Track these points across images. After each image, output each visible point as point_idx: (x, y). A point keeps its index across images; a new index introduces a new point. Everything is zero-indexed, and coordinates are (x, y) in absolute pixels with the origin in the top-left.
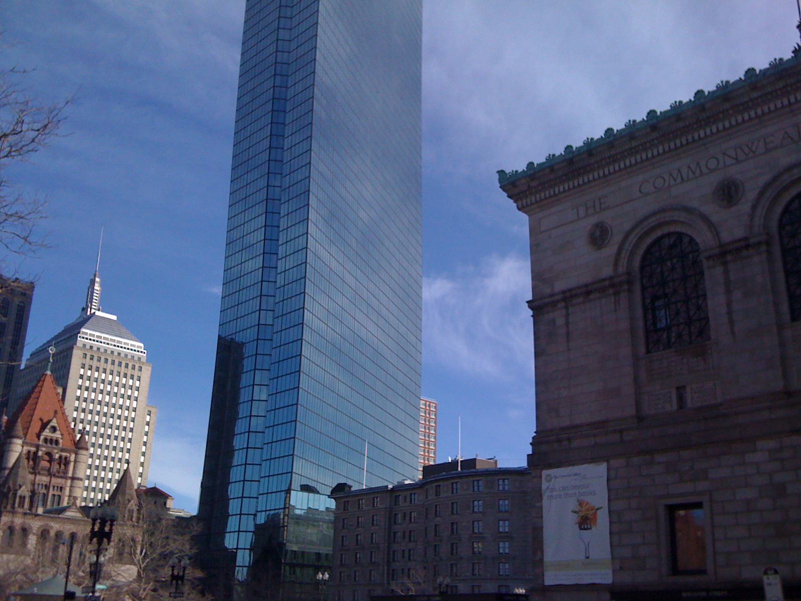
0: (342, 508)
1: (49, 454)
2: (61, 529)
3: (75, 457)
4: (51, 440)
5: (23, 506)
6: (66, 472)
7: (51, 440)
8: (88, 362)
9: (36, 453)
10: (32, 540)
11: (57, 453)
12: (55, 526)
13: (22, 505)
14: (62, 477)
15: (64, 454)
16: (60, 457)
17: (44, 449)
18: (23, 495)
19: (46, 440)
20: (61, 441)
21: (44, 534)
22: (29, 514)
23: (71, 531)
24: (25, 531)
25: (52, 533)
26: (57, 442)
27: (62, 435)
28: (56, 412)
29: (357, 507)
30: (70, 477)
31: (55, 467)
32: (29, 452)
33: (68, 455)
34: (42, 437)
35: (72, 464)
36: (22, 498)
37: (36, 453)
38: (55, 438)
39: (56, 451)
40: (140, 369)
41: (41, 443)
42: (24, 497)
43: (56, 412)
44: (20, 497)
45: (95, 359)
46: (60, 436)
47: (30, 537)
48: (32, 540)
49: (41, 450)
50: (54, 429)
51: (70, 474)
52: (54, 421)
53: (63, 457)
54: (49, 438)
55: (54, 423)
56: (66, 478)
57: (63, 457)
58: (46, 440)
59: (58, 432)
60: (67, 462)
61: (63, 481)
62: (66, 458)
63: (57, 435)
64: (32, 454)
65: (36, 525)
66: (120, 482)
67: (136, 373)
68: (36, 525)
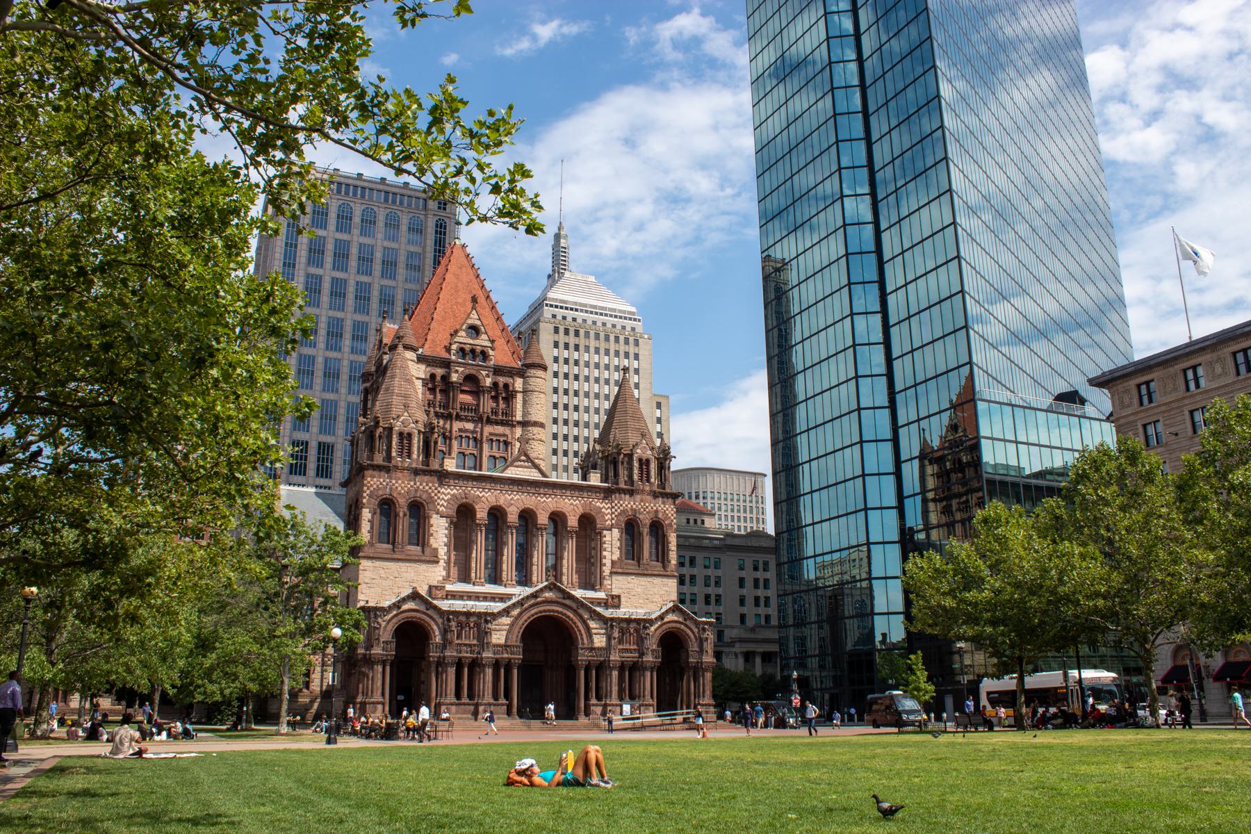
0: (1136, 401)
1: (471, 379)
2: (501, 502)
3: (524, 383)
4: (473, 351)
5: (409, 456)
6: (509, 412)
7: (473, 351)
8: (562, 338)
9: (445, 378)
10: (440, 531)
11: (488, 376)
12: (485, 499)
13: (406, 450)
14: (502, 423)
15: (501, 380)
16: (495, 384)
17: (461, 369)
18: (406, 430)
19: (462, 350)
20: (491, 352)
21: (463, 515)
22: (425, 472)
23: (522, 507)
24: (418, 510)
25: (482, 514)
26: (485, 356)
27: (493, 342)
28: (474, 300)
29: (1183, 387)
30: (519, 423)
31: (487, 405)
32: (433, 376)
33: (510, 380)
34: (454, 347)
35: (520, 397)
36: (405, 437)
37: (445, 378)
38: (479, 349)
39: (484, 373)
40: (637, 343)
41: (453, 358)
42: (410, 435)
43: (474, 300)
44: (401, 434)
45: (572, 333)
46: (488, 344)
47: (433, 521)
48: (440, 531)
49: (457, 371)
50: (475, 330)
51: (519, 417)
52: (474, 315)
53: (501, 385)
54: (467, 348)
55: (474, 320)
56: (510, 424)
57: (501, 385)
58: (462, 350)
59: (484, 337)
60: (510, 396)
61: (507, 430)
62: (506, 386)
63: (483, 341)
64: (438, 378)
65: (446, 496)
66: (611, 413)
67: (632, 349)
68: (446, 496)
